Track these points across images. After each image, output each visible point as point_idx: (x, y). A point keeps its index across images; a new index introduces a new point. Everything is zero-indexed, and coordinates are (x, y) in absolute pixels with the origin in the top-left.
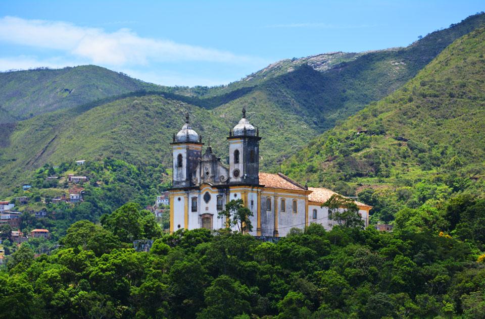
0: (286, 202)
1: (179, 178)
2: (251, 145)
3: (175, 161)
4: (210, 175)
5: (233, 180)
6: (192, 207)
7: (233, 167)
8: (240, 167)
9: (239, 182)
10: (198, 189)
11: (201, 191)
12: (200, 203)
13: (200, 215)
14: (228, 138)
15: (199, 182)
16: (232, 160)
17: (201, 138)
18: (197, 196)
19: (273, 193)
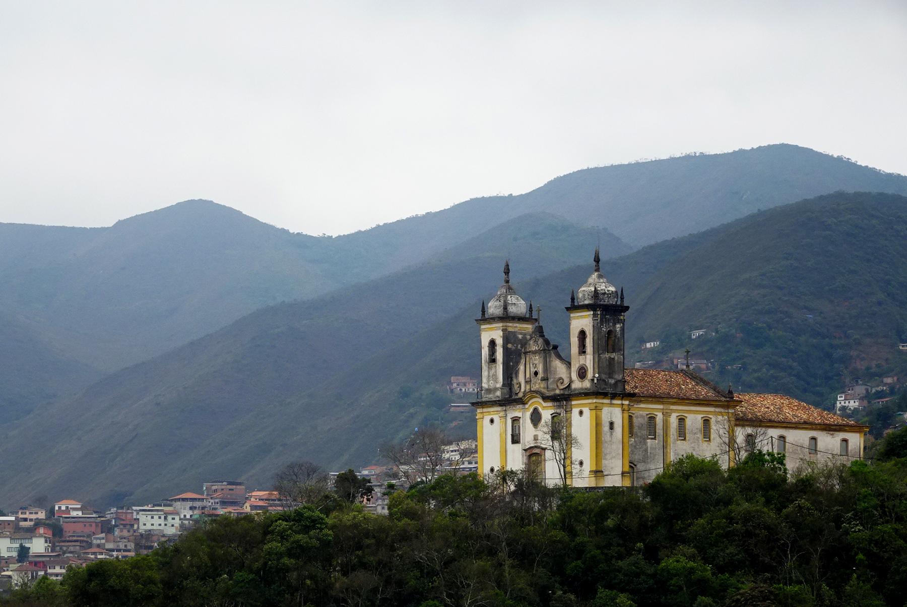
0: (688, 422)
2: (607, 321)
3: (485, 352)
4: (540, 375)
5: (577, 385)
6: (512, 435)
7: (577, 362)
8: (588, 360)
10: (522, 402)
11: (527, 406)
12: (524, 427)
14: (568, 309)
15: (523, 390)
16: (575, 349)
17: (531, 309)
18: (518, 414)
19: (661, 407)
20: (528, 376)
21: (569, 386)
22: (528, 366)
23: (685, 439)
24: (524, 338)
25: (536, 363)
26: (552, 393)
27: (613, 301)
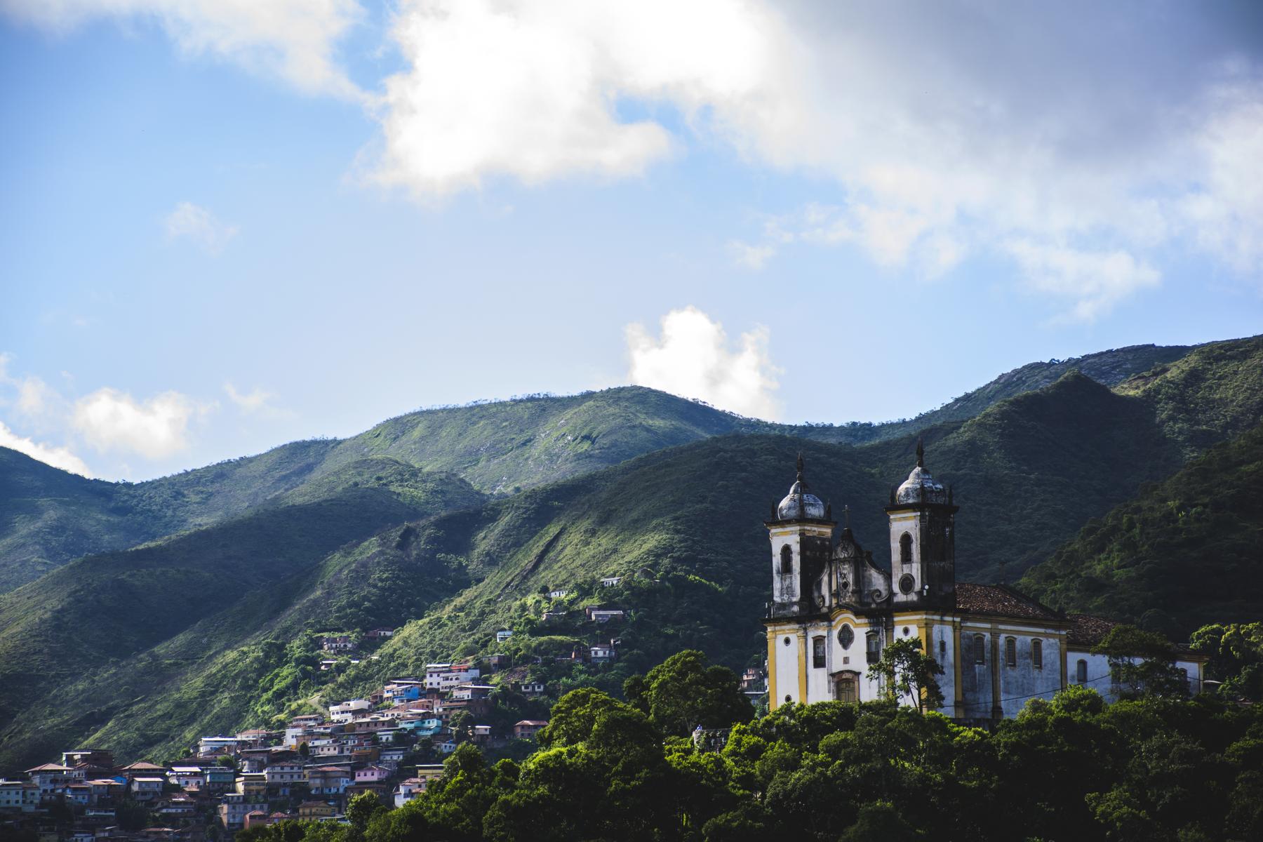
0: (1018, 644)
1: (786, 597)
3: (777, 561)
4: (851, 588)
5: (900, 598)
6: (815, 658)
8: (915, 570)
9: (912, 602)
10: (828, 618)
13: (833, 675)
15: (827, 604)
16: (896, 556)
17: (828, 511)
18: (825, 633)
19: (989, 626)
20: (834, 587)
22: (834, 577)
23: (1014, 665)
27: (941, 500)
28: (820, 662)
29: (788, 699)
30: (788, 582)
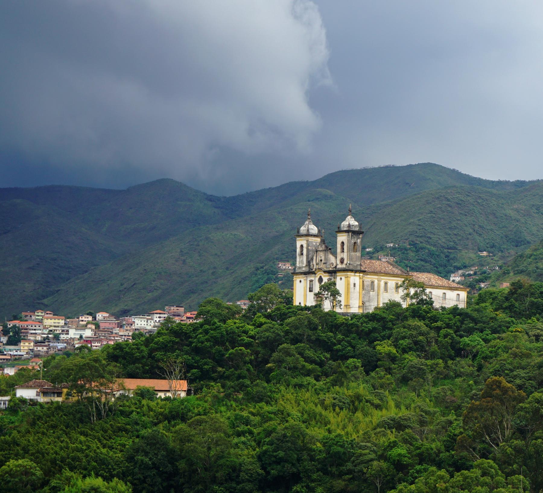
0: (389, 285)
1: (301, 264)
3: (298, 250)
4: (323, 262)
5: (339, 266)
6: (310, 288)
8: (345, 255)
10: (314, 273)
14: (337, 232)
17: (319, 231)
18: (313, 279)
19: (377, 277)
21: (336, 267)
24: (316, 244)
25: (322, 255)
26: (328, 270)
27: (357, 229)
28: (311, 291)
29: (300, 303)
30: (301, 259)
